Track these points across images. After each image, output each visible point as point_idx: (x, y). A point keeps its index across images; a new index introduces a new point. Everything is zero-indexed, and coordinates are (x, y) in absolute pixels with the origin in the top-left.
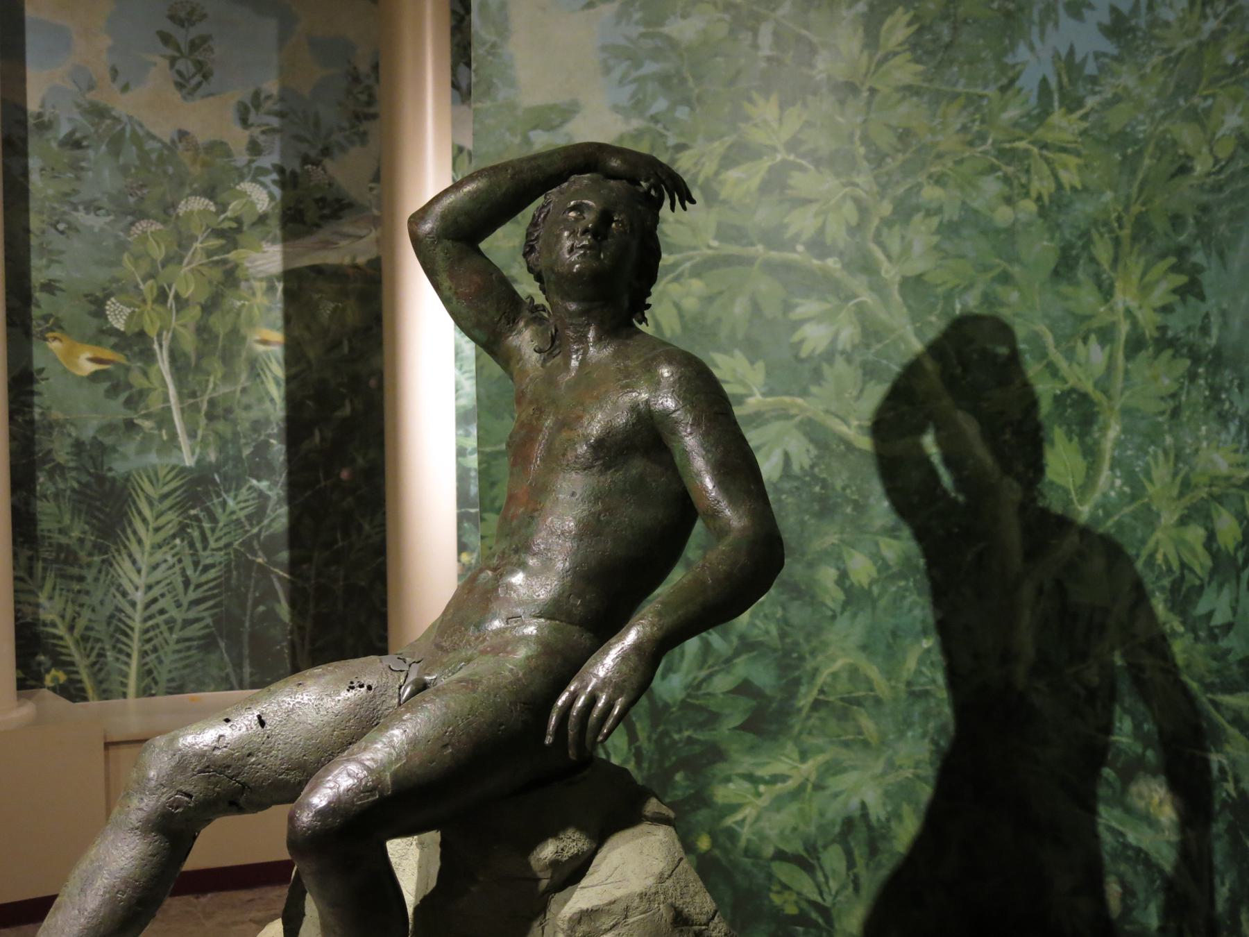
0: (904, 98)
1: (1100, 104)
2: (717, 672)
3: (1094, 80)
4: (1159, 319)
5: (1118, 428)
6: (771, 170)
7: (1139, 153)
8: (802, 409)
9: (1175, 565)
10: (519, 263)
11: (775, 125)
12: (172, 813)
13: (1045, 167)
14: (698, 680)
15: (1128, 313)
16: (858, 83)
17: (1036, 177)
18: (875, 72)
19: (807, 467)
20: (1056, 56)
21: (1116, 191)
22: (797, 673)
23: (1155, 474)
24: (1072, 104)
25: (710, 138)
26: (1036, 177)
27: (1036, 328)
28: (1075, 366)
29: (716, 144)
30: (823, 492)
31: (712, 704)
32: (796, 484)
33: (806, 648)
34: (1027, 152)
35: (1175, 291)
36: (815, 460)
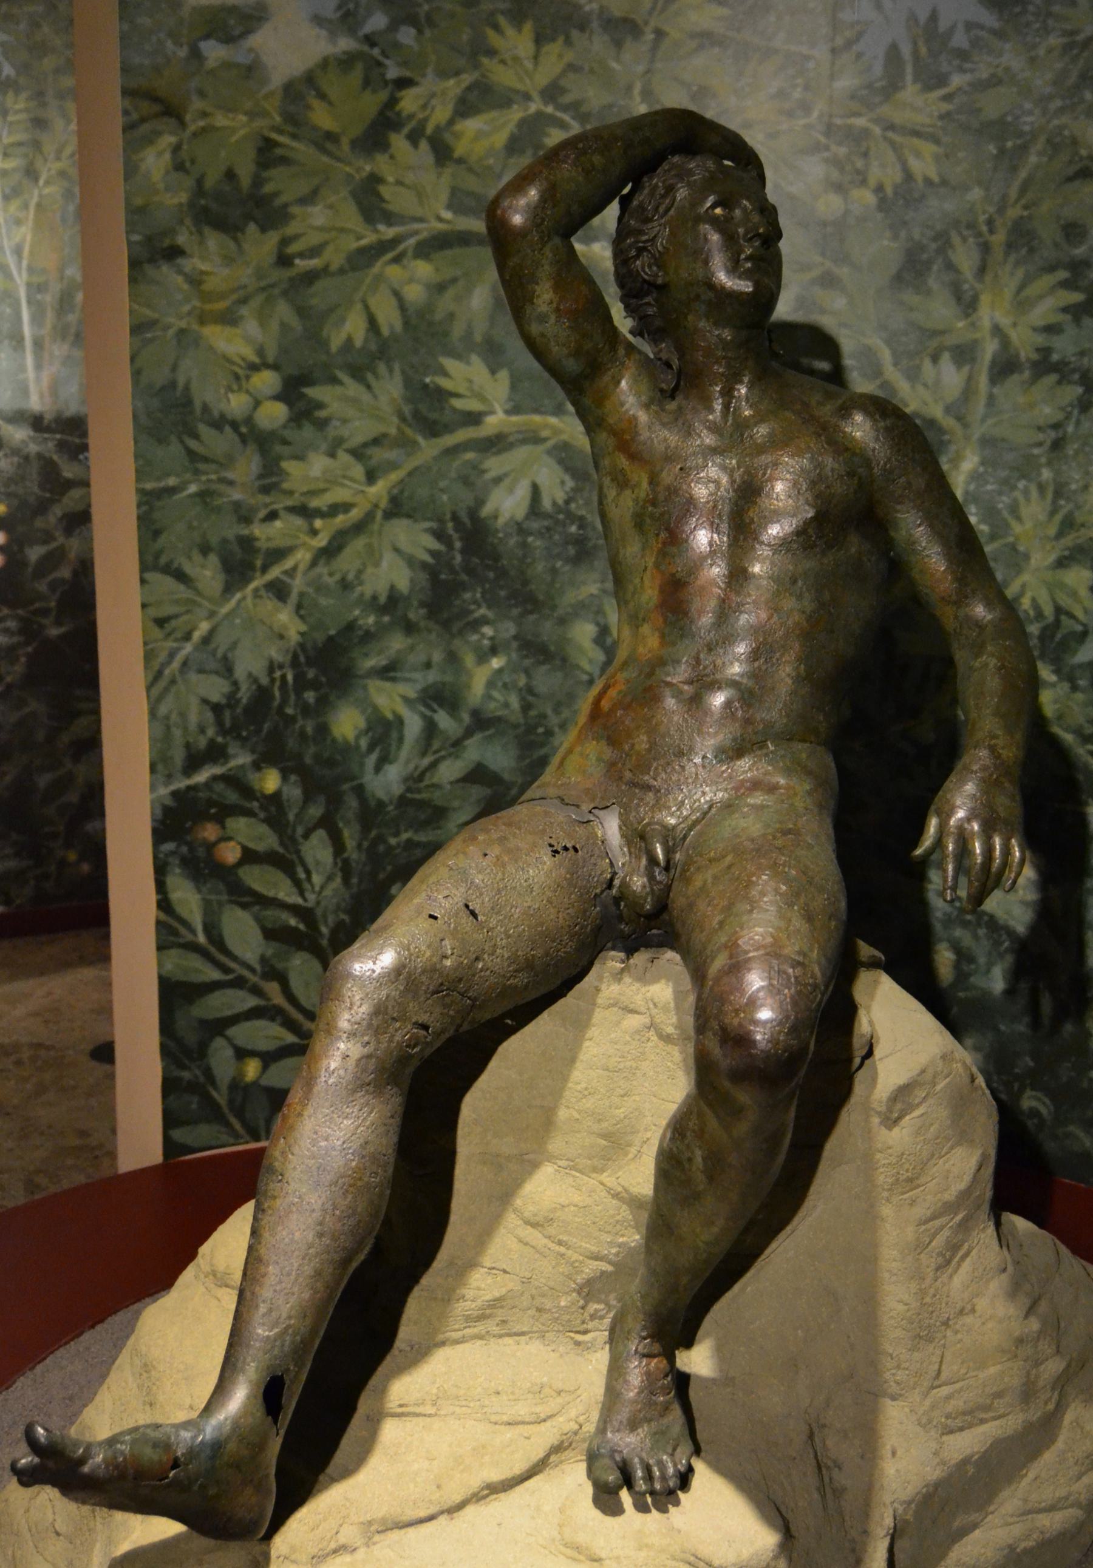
0: (701, 47)
1: (970, 84)
2: (443, 758)
3: (962, 55)
4: (1040, 340)
5: (976, 459)
6: (522, 123)
7: (1024, 148)
8: (556, 431)
9: (1048, 611)
10: (188, 228)
11: (529, 65)
12: (410, 1054)
13: (890, 153)
14: (420, 770)
15: (997, 330)
16: (640, 22)
17: (876, 163)
18: (663, 10)
19: (560, 502)
20: (912, 18)
21: (987, 189)
22: (543, 752)
23: (1025, 511)
24: (933, 80)
25: (443, 74)
26: (876, 163)
27: (869, 342)
28: (920, 389)
29: (452, 82)
30: (581, 532)
31: (437, 797)
32: (546, 523)
33: (554, 720)
34: (866, 133)
35: (1065, 310)
36: (571, 495)
